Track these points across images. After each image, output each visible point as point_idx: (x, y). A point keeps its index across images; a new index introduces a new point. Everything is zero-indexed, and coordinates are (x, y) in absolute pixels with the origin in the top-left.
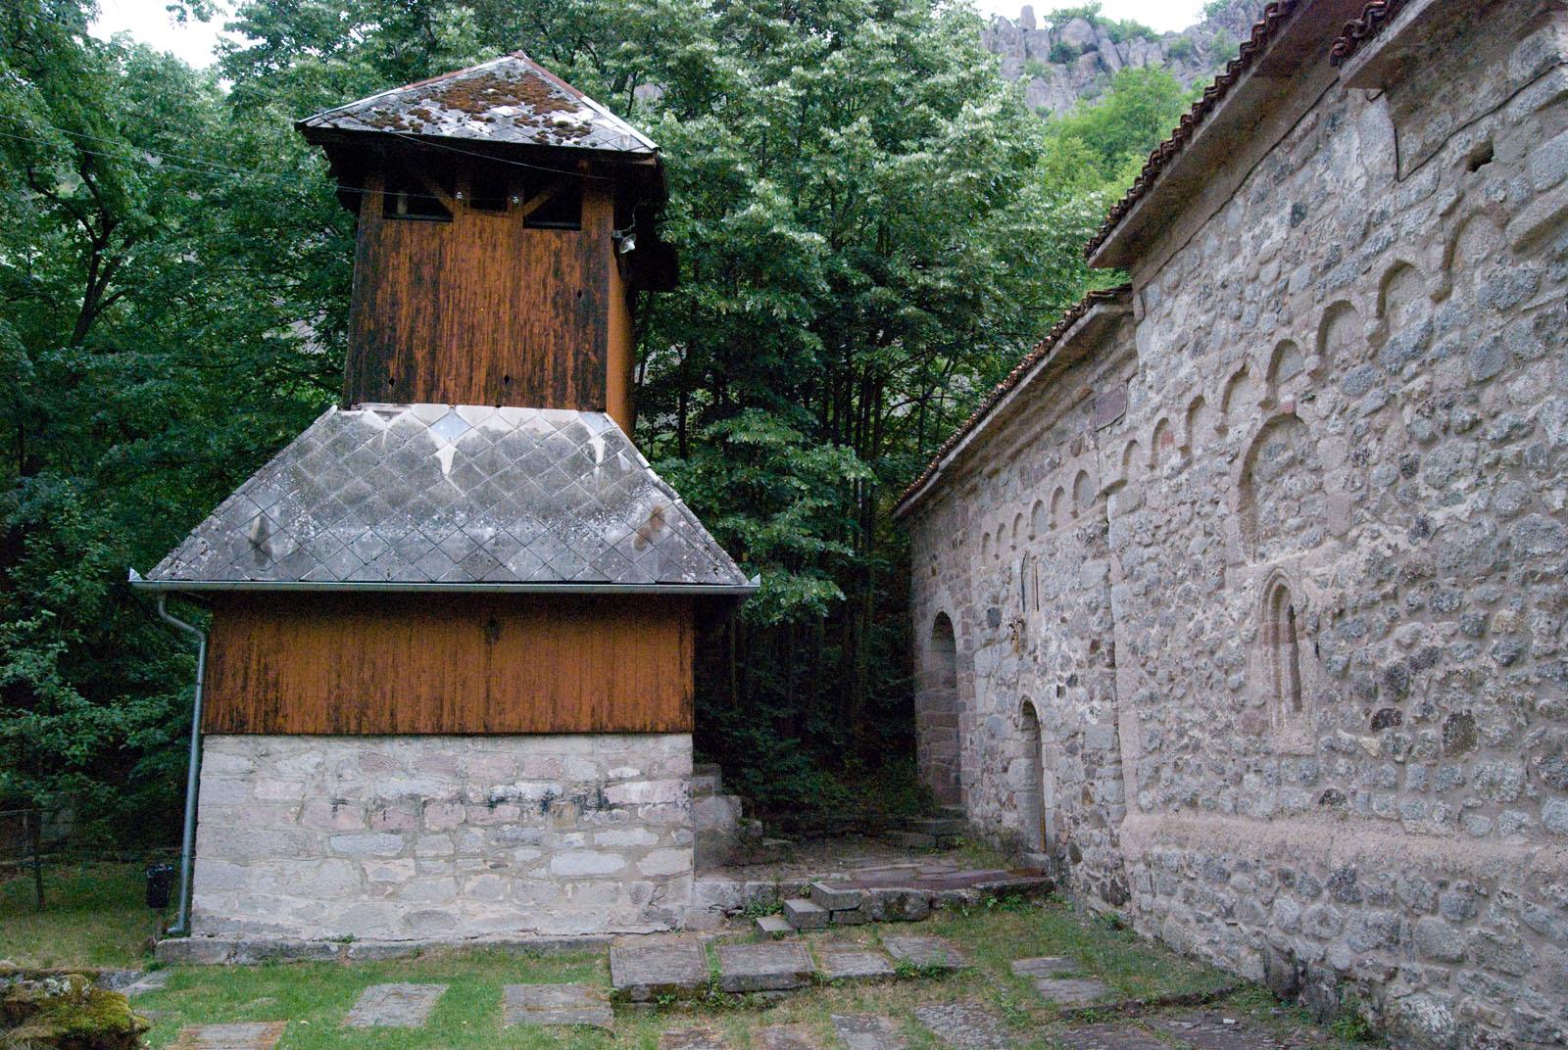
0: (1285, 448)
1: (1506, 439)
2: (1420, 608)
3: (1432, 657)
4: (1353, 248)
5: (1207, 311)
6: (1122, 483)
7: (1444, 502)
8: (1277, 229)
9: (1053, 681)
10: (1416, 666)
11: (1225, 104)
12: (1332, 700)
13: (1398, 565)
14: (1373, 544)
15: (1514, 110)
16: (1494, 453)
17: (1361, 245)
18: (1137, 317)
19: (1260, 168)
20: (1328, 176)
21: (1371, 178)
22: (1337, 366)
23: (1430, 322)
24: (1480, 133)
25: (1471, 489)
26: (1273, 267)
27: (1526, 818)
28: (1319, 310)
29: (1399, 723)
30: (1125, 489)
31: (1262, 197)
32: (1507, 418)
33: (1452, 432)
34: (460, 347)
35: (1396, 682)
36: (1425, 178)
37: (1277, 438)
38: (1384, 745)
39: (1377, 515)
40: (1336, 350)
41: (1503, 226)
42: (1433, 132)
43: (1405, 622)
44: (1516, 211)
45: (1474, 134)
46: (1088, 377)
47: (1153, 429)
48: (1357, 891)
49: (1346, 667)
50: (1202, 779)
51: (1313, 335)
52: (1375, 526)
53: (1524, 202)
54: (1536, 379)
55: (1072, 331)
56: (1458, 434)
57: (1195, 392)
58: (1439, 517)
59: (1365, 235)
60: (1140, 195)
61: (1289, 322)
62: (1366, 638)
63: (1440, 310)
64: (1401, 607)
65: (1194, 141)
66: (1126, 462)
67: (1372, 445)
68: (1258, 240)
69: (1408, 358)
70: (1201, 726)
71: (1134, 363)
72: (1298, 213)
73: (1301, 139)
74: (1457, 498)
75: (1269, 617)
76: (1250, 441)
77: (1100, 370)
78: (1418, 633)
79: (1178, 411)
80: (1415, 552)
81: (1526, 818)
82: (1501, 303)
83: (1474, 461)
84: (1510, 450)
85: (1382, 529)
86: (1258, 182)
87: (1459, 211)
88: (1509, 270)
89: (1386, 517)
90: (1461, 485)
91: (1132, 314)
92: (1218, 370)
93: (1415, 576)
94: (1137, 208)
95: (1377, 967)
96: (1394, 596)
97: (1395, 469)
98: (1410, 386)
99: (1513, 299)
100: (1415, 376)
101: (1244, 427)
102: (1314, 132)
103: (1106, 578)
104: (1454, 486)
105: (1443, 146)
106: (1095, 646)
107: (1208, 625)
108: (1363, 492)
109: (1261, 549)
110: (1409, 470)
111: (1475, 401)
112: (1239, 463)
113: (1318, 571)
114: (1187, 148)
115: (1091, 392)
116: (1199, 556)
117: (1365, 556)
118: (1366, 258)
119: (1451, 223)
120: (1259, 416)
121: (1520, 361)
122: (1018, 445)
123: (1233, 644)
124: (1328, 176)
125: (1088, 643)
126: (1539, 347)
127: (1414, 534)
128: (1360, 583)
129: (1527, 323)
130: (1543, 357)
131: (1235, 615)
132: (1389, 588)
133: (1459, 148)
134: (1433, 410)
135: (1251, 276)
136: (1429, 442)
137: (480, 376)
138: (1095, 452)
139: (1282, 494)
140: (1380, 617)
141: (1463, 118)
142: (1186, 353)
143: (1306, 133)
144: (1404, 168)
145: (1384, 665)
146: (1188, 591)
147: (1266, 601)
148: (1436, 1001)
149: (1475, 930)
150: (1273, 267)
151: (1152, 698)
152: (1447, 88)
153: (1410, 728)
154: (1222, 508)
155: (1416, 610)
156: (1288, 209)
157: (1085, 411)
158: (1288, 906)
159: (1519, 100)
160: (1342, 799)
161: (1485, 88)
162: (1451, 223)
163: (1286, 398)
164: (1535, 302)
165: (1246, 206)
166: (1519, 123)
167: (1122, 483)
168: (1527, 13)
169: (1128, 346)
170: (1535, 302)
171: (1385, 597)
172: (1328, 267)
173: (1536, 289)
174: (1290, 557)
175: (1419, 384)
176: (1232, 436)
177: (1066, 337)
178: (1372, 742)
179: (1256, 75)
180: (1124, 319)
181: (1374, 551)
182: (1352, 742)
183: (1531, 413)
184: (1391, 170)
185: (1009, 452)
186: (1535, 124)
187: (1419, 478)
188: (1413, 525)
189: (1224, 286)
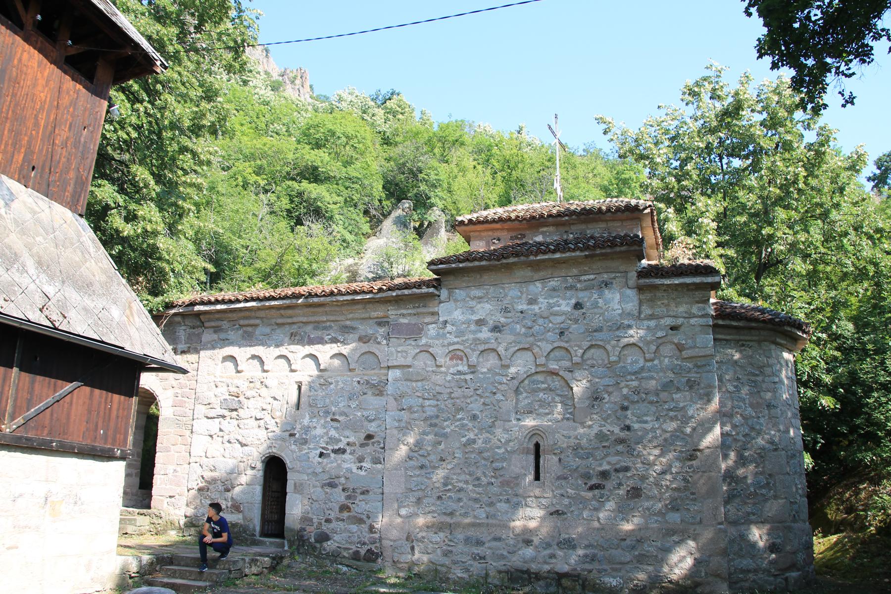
0: (543, 383)
1: (671, 410)
2: (622, 452)
3: (627, 469)
4: (610, 330)
5: (506, 318)
6: (409, 366)
7: (640, 422)
8: (565, 306)
9: (315, 449)
10: (617, 471)
11: (564, 255)
12: (565, 478)
13: (613, 438)
14: (600, 429)
15: (693, 321)
16: (665, 413)
17: (615, 331)
18: (442, 298)
19: (556, 279)
20: (600, 301)
21: (623, 312)
22: (588, 365)
23: (643, 366)
24: (680, 321)
25: (652, 421)
26: (559, 319)
27: (660, 519)
28: (586, 344)
29: (604, 488)
30: (411, 370)
31: (554, 289)
32: (672, 405)
33: (646, 402)
34: (11, 131)
35: (604, 475)
36: (652, 323)
37: (540, 378)
38: (594, 496)
39: (605, 420)
40: (589, 359)
41: (680, 351)
42: (658, 311)
43: (612, 456)
44: (688, 349)
46: (392, 312)
47: (447, 351)
48: (575, 545)
49: (577, 468)
50: (461, 504)
51: (581, 351)
52: (603, 423)
53: (691, 348)
54: (685, 397)
56: (649, 403)
57: (491, 346)
58: (636, 426)
59: (618, 329)
60: (481, 259)
61: (567, 342)
62: (591, 459)
63: (649, 364)
64: (612, 450)
65: (538, 258)
66: (414, 358)
67: (606, 396)
68: (550, 306)
69: (630, 374)
70: (466, 482)
71: (436, 317)
72: (578, 306)
73: (585, 281)
74: (646, 422)
76: (525, 376)
77: (404, 312)
78: (620, 460)
79: (473, 350)
80: (623, 435)
81: (660, 519)
82: (675, 371)
83: (655, 413)
84: (672, 414)
85: (606, 424)
86: (553, 283)
87: (664, 339)
88: (680, 363)
89: (609, 421)
90: (649, 419)
91: (439, 296)
92: (511, 343)
93: (622, 441)
94: (484, 263)
95: (583, 570)
96: (609, 447)
97: (617, 407)
98: (628, 383)
100: (632, 380)
101: (522, 370)
102: (592, 282)
104: (645, 418)
106: (369, 437)
107: (480, 441)
109: (518, 417)
110: (625, 409)
111: (657, 395)
112: (516, 382)
113: (565, 432)
115: (388, 317)
116: (478, 413)
118: (618, 337)
119: (660, 341)
120: (533, 368)
121: (678, 389)
122: (295, 320)
123: (502, 450)
124: (600, 301)
125: (363, 436)
126: (687, 388)
127: (622, 429)
128: (591, 440)
129: (684, 380)
130: (687, 391)
131: (503, 440)
132: (606, 444)
133: (669, 321)
134: (639, 393)
135: (545, 315)
136: (633, 402)
137: (19, 158)
138: (386, 346)
139: (537, 399)
140: (599, 454)
141: (671, 313)
142: (485, 329)
143: (589, 280)
144: (642, 316)
145: (601, 469)
146: (463, 426)
148: (614, 577)
149: (636, 553)
150: (559, 319)
151: (422, 467)
152: (666, 301)
153: (610, 490)
154: (499, 396)
155: (618, 453)
156: (573, 301)
157: (380, 324)
158: (529, 552)
159: (696, 319)
160: (564, 513)
161: (682, 309)
162: (660, 341)
163: (553, 366)
165: (543, 289)
166: (694, 325)
167: (409, 366)
169: (436, 309)
171: (604, 447)
172: (595, 331)
173: (689, 372)
174: (546, 423)
175: (635, 384)
176: (513, 370)
177: (399, 292)
178: (589, 494)
179: (585, 255)
181: (601, 431)
182: (575, 493)
183: (682, 405)
184: (636, 313)
185: (280, 321)
186: (700, 328)
187: (629, 412)
188: (622, 426)
189: (522, 312)
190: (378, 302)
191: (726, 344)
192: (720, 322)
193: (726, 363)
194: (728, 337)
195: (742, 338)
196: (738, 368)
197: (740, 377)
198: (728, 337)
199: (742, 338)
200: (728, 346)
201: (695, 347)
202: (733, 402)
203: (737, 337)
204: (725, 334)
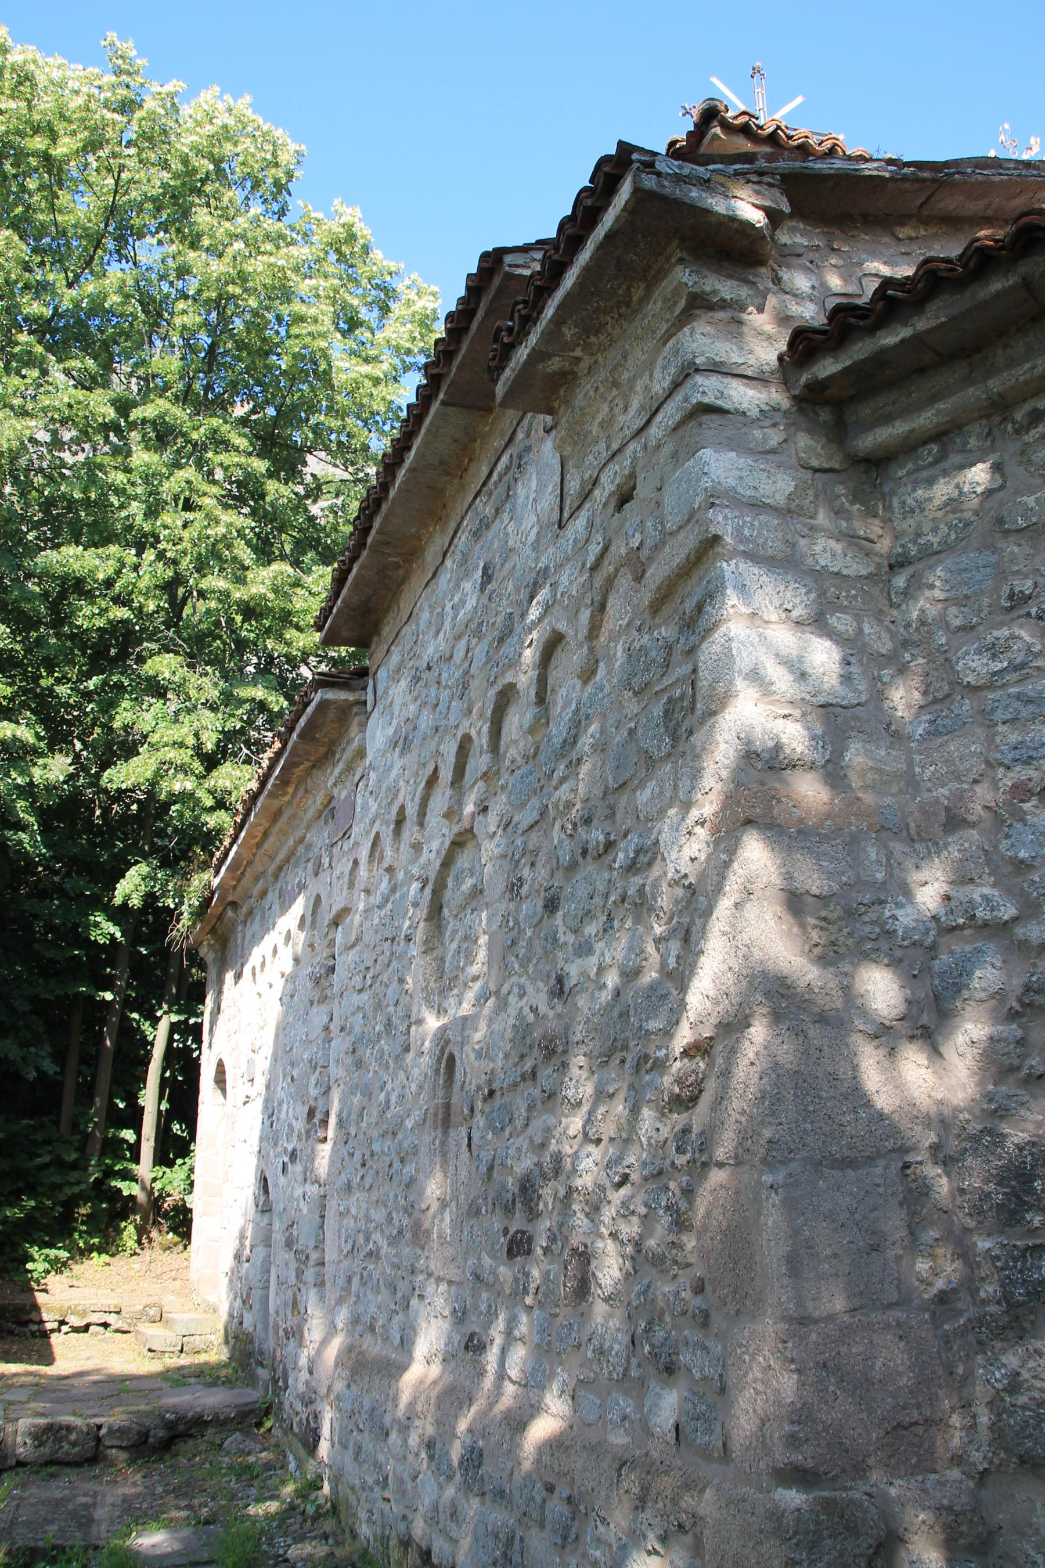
15: (655, 432)
18: (369, 708)
21: (541, 527)
33: (589, 858)
40: (507, 747)
45: (621, 464)
55: (302, 722)
75: (440, 1093)
76: (438, 863)
91: (365, 703)
92: (417, 773)
99: (646, 678)
101: (435, 845)
103: (327, 1028)
105: (595, 482)
106: (311, 1114)
108: (514, 933)
110: (551, 905)
114: (392, 493)
117: (511, 1021)
119: (599, 580)
125: (306, 1109)
144: (566, 515)
147: (437, 1071)
164: (666, 682)
168: (670, 309)
170: (666, 682)
180: (355, 710)
189: (429, 668)
190: (314, 766)
191: (943, 456)
192: (827, 367)
193: (946, 548)
194: (925, 420)
195: (995, 385)
196: (1011, 547)
197: (1026, 586)
198: (925, 420)
199: (995, 385)
200: (954, 459)
201: (666, 536)
202: (990, 739)
203: (973, 394)
204: (905, 412)
